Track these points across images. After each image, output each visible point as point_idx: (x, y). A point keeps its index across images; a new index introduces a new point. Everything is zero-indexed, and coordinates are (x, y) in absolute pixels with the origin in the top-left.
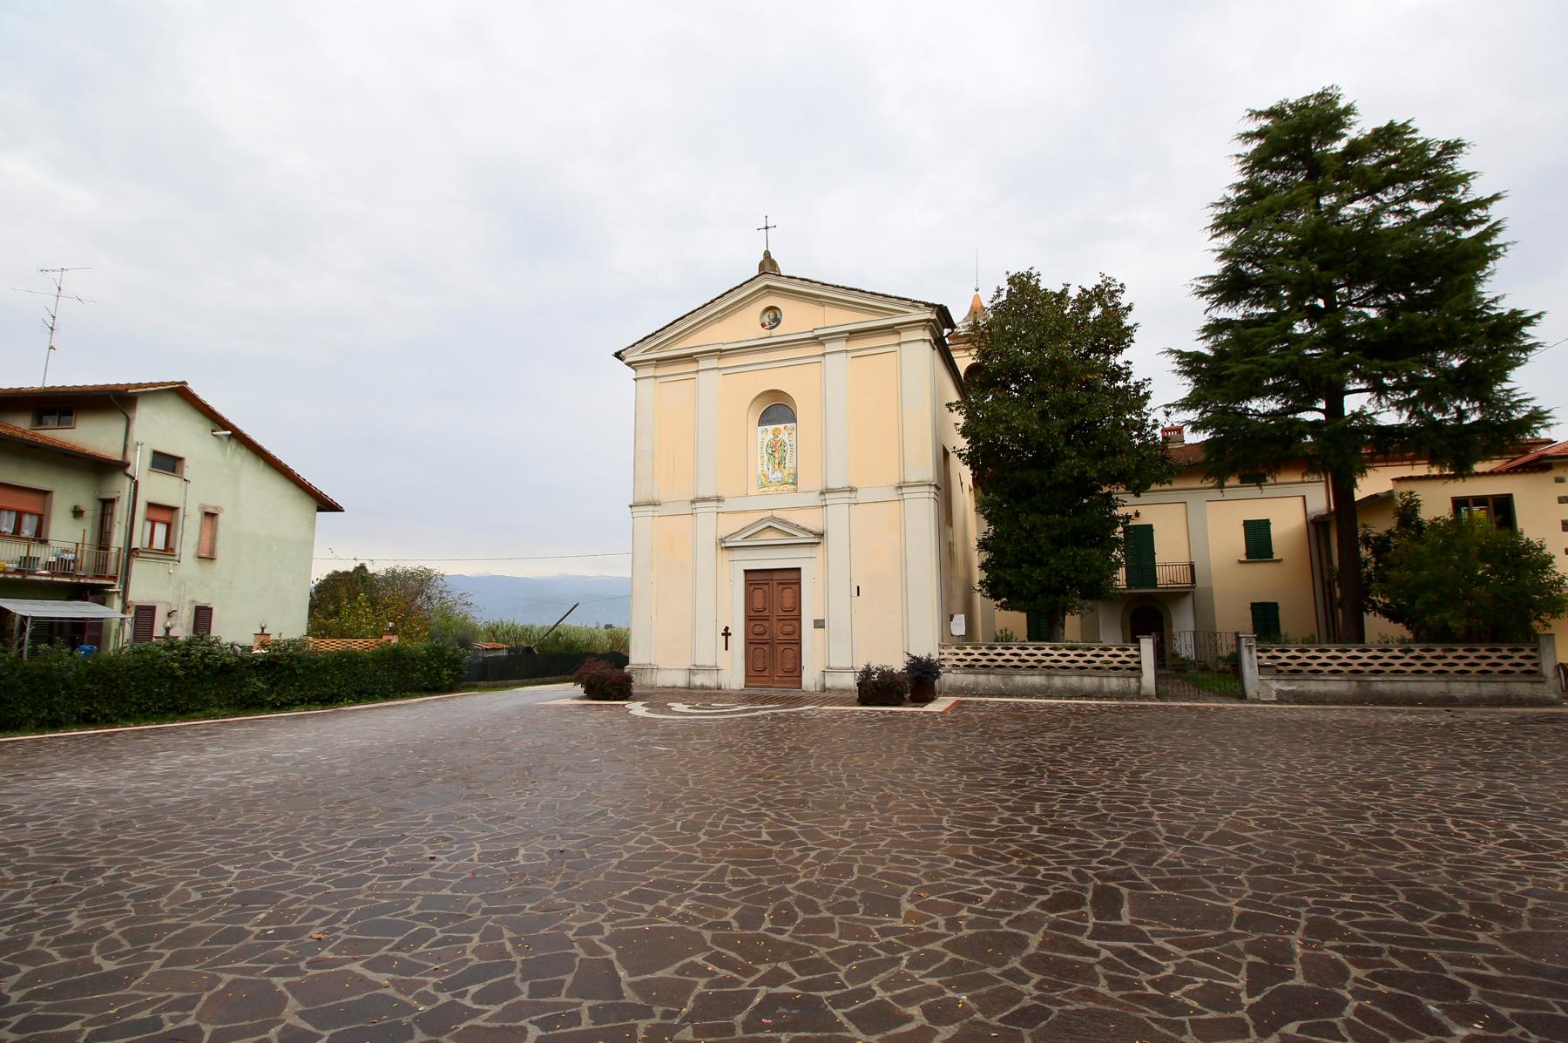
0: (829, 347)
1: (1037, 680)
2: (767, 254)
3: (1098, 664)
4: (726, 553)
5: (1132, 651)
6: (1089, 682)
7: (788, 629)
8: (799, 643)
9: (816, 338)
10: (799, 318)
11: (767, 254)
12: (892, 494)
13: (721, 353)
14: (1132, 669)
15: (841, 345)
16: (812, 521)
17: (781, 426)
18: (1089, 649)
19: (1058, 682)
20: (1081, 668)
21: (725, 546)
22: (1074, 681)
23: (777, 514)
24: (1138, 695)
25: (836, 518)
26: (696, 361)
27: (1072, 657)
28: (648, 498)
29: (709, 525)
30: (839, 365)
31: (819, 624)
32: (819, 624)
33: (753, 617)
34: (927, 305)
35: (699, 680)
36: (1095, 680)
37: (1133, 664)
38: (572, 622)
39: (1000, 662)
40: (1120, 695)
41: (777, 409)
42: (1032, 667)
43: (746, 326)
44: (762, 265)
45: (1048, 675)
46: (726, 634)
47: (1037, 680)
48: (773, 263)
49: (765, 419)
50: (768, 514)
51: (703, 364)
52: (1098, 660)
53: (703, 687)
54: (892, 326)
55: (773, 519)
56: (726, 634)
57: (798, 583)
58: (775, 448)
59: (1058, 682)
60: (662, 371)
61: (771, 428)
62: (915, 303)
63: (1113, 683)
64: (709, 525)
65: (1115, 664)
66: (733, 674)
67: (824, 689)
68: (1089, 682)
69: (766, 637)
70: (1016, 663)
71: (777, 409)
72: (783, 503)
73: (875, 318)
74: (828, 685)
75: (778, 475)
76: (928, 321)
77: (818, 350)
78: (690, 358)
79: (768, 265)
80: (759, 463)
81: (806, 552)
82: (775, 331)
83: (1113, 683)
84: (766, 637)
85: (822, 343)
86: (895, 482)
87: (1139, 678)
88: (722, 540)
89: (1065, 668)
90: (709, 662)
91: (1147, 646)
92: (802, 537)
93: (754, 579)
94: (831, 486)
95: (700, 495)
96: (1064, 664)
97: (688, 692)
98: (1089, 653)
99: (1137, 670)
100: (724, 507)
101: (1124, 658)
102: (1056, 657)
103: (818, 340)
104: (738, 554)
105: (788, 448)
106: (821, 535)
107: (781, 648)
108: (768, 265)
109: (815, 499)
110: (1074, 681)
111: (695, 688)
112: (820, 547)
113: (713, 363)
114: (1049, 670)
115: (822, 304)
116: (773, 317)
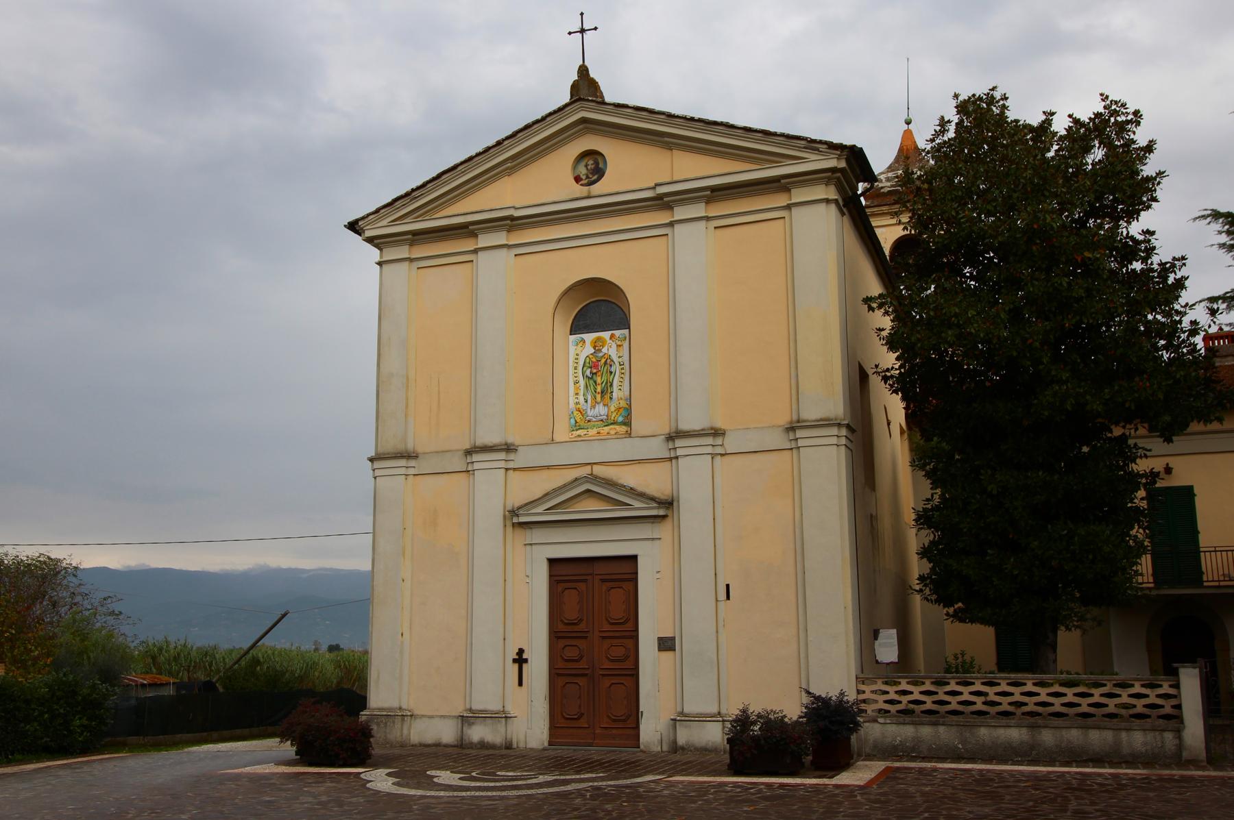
0: (680, 213)
1: (1015, 734)
2: (583, 71)
3: (1111, 709)
4: (520, 532)
5: (1166, 689)
6: (1098, 738)
7: (618, 652)
8: (634, 674)
9: (660, 197)
10: (631, 169)
11: (583, 71)
12: (777, 439)
13: (511, 223)
14: (1167, 717)
15: (698, 210)
16: (652, 480)
17: (606, 335)
18: (1098, 685)
19: (1047, 737)
20: (1085, 715)
21: (518, 520)
22: (1074, 735)
23: (599, 471)
24: (1178, 758)
25: (693, 478)
26: (474, 235)
27: (1070, 698)
28: (401, 447)
29: (494, 490)
30: (695, 243)
31: (666, 644)
32: (666, 644)
33: (561, 633)
34: (832, 146)
35: (478, 733)
36: (1108, 735)
37: (1168, 710)
38: (278, 641)
39: (954, 706)
40: (1148, 759)
41: (598, 307)
42: (1006, 714)
43: (550, 182)
44: (575, 87)
45: (1032, 727)
46: (520, 660)
47: (1015, 734)
48: (593, 86)
49: (579, 325)
50: (585, 471)
51: (484, 240)
52: (1112, 702)
53: (483, 745)
54: (776, 180)
55: (593, 478)
56: (520, 660)
57: (633, 579)
58: (597, 368)
59: (1047, 737)
60: (418, 252)
61: (589, 337)
62: (812, 145)
63: (1137, 740)
64: (494, 490)
65: (1140, 709)
66: (530, 723)
67: (675, 748)
68: (1098, 738)
69: (583, 664)
70: (979, 706)
71: (598, 307)
72: (605, 452)
73: (751, 168)
74: (682, 740)
75: (601, 410)
76: (833, 170)
77: (662, 217)
78: (465, 230)
79: (585, 87)
80: (572, 393)
81: (646, 530)
82: (597, 188)
83: (1137, 740)
84: (583, 664)
85: (669, 207)
86: (784, 419)
87: (1178, 732)
88: (514, 512)
89: (1058, 715)
90: (494, 706)
91: (1190, 683)
92: (639, 508)
94: (684, 426)
95: (479, 442)
96: (1058, 708)
97: (461, 754)
98: (1097, 692)
99: (1175, 719)
100: (520, 459)
101: (1152, 700)
102: (1043, 698)
103: (662, 202)
104: (538, 535)
105: (616, 368)
106: (669, 504)
107: (606, 682)
108: (585, 87)
109: (657, 447)
110: (1074, 735)
111: (471, 745)
112: (669, 521)
113: (500, 238)
114: (1034, 719)
115: (669, 147)
116: (593, 167)
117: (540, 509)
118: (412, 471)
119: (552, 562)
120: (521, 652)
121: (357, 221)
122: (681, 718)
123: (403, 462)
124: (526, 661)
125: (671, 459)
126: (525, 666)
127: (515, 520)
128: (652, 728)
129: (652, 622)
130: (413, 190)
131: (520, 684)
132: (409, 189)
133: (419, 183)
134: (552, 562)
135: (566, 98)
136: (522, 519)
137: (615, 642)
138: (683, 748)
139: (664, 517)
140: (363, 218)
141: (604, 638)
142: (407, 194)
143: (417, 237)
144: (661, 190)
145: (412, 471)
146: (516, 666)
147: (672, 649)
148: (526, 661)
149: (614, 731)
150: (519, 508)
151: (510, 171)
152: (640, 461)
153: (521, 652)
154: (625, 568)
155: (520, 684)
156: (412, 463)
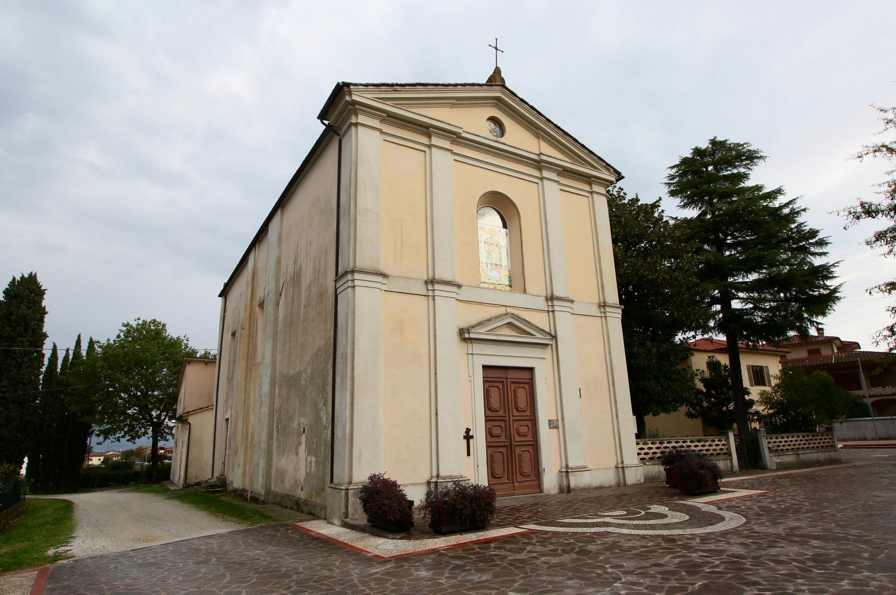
2: (497, 71)
4: (464, 345)
5: (724, 442)
9: (538, 162)
10: (517, 137)
11: (497, 71)
12: (595, 311)
13: (455, 137)
14: (725, 454)
23: (509, 310)
25: (566, 325)
29: (452, 314)
31: (553, 425)
33: (493, 416)
37: (725, 451)
50: (502, 310)
55: (513, 316)
56: (468, 437)
60: (386, 128)
62: (608, 166)
72: (516, 299)
78: (426, 129)
82: (501, 140)
93: (494, 376)
100: (464, 294)
103: (539, 164)
104: (477, 348)
109: (542, 304)
113: (447, 144)
115: (538, 136)
117: (483, 330)
118: (384, 287)
119: (484, 367)
120: (468, 430)
121: (347, 85)
122: (566, 472)
123: (379, 279)
124: (472, 437)
125: (548, 312)
126: (471, 441)
127: (467, 336)
128: (550, 481)
129: (545, 411)
130: (397, 85)
131: (469, 454)
132: (395, 82)
133: (403, 82)
134: (484, 367)
135: (484, 82)
136: (472, 336)
137: (521, 423)
138: (574, 490)
139: (547, 345)
140: (355, 85)
141: (516, 420)
142: (392, 85)
143: (391, 118)
144: (543, 157)
145: (384, 287)
146: (465, 441)
147: (557, 427)
148: (472, 437)
149: (525, 484)
150: (473, 327)
151: (453, 106)
152: (532, 309)
153: (468, 430)
154: (526, 375)
155: (469, 454)
156: (385, 281)
